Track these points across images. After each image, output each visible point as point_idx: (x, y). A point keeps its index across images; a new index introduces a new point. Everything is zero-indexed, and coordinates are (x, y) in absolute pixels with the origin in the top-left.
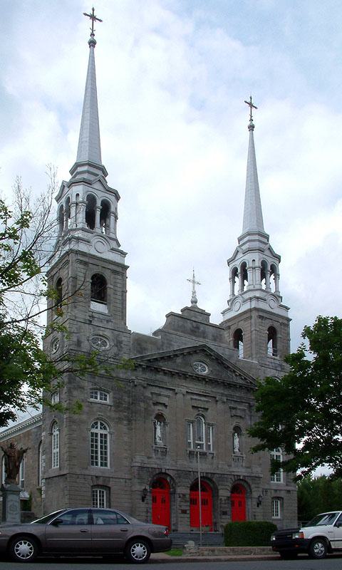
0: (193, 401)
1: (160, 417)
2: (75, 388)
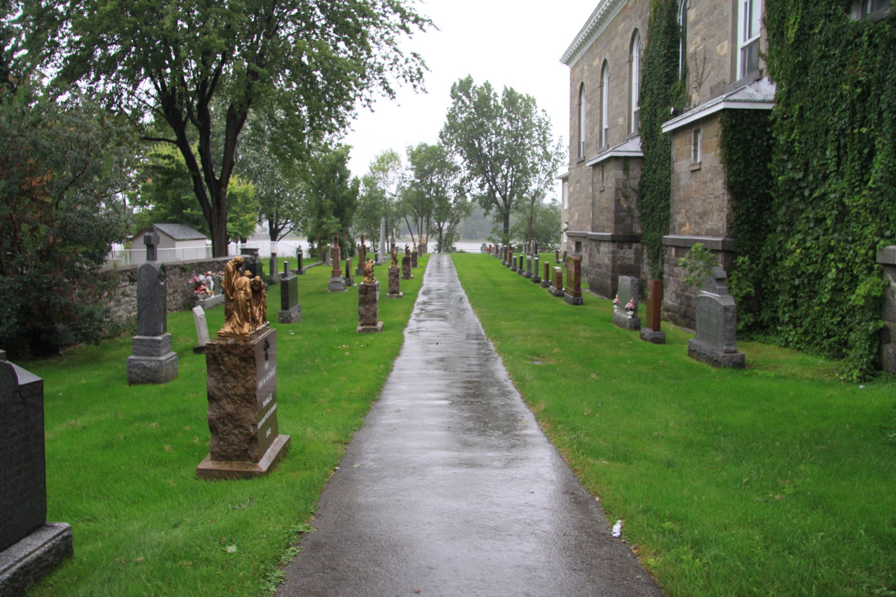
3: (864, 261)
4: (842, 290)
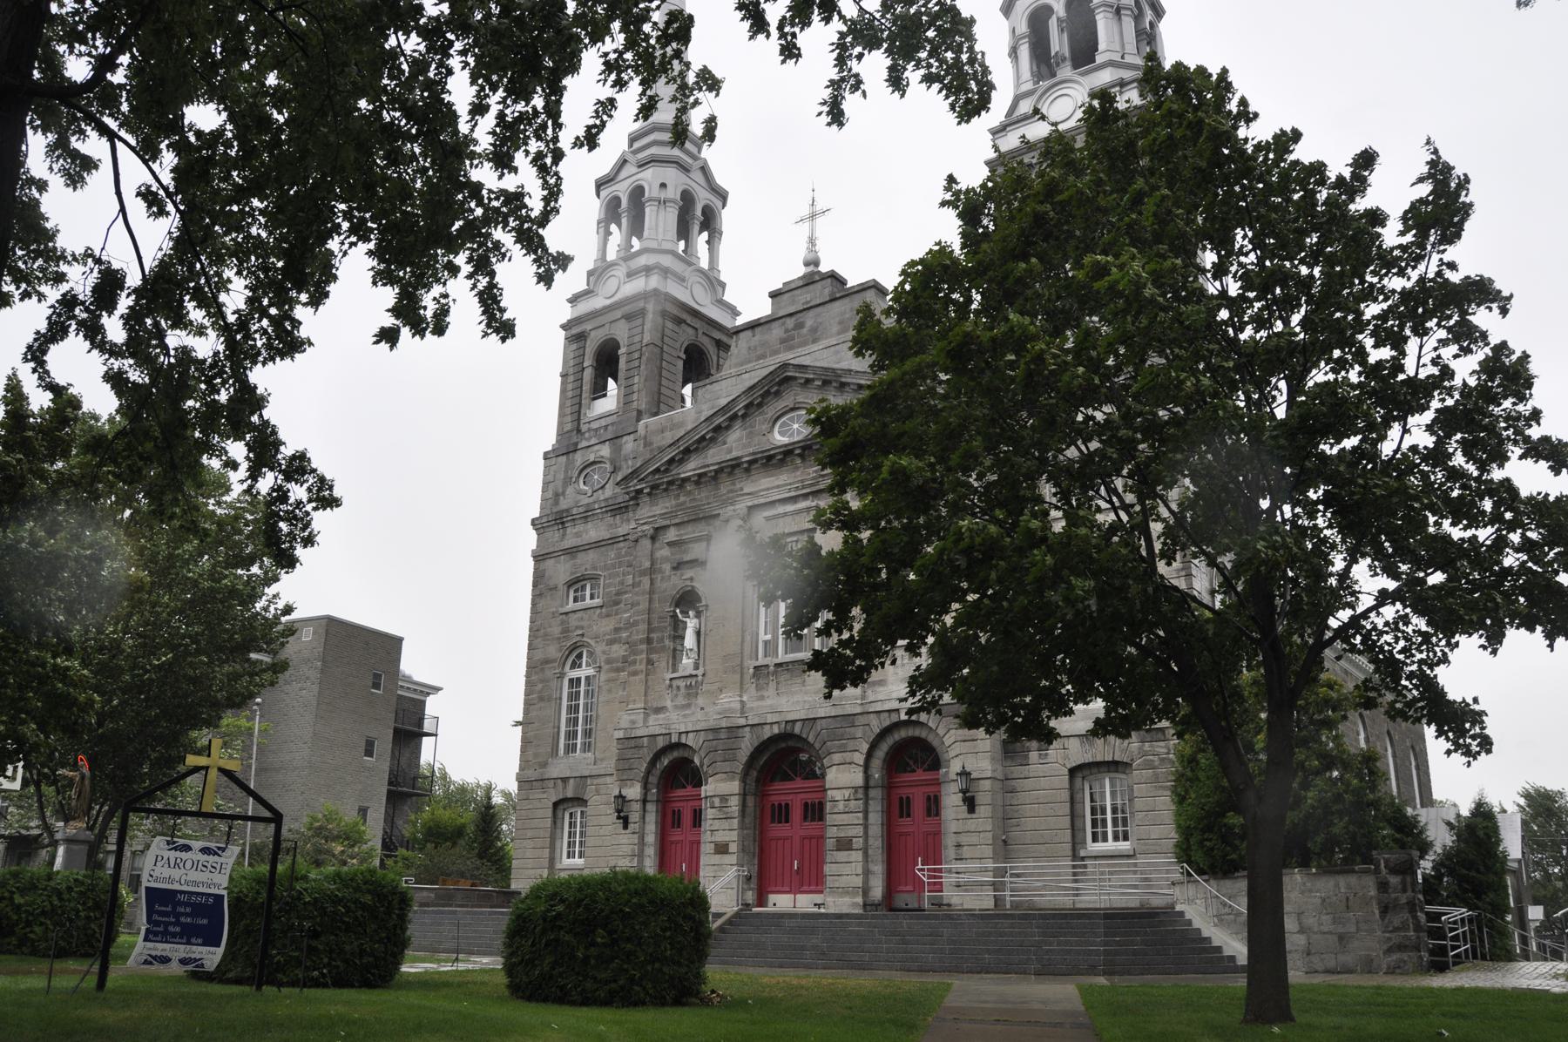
1: (687, 600)
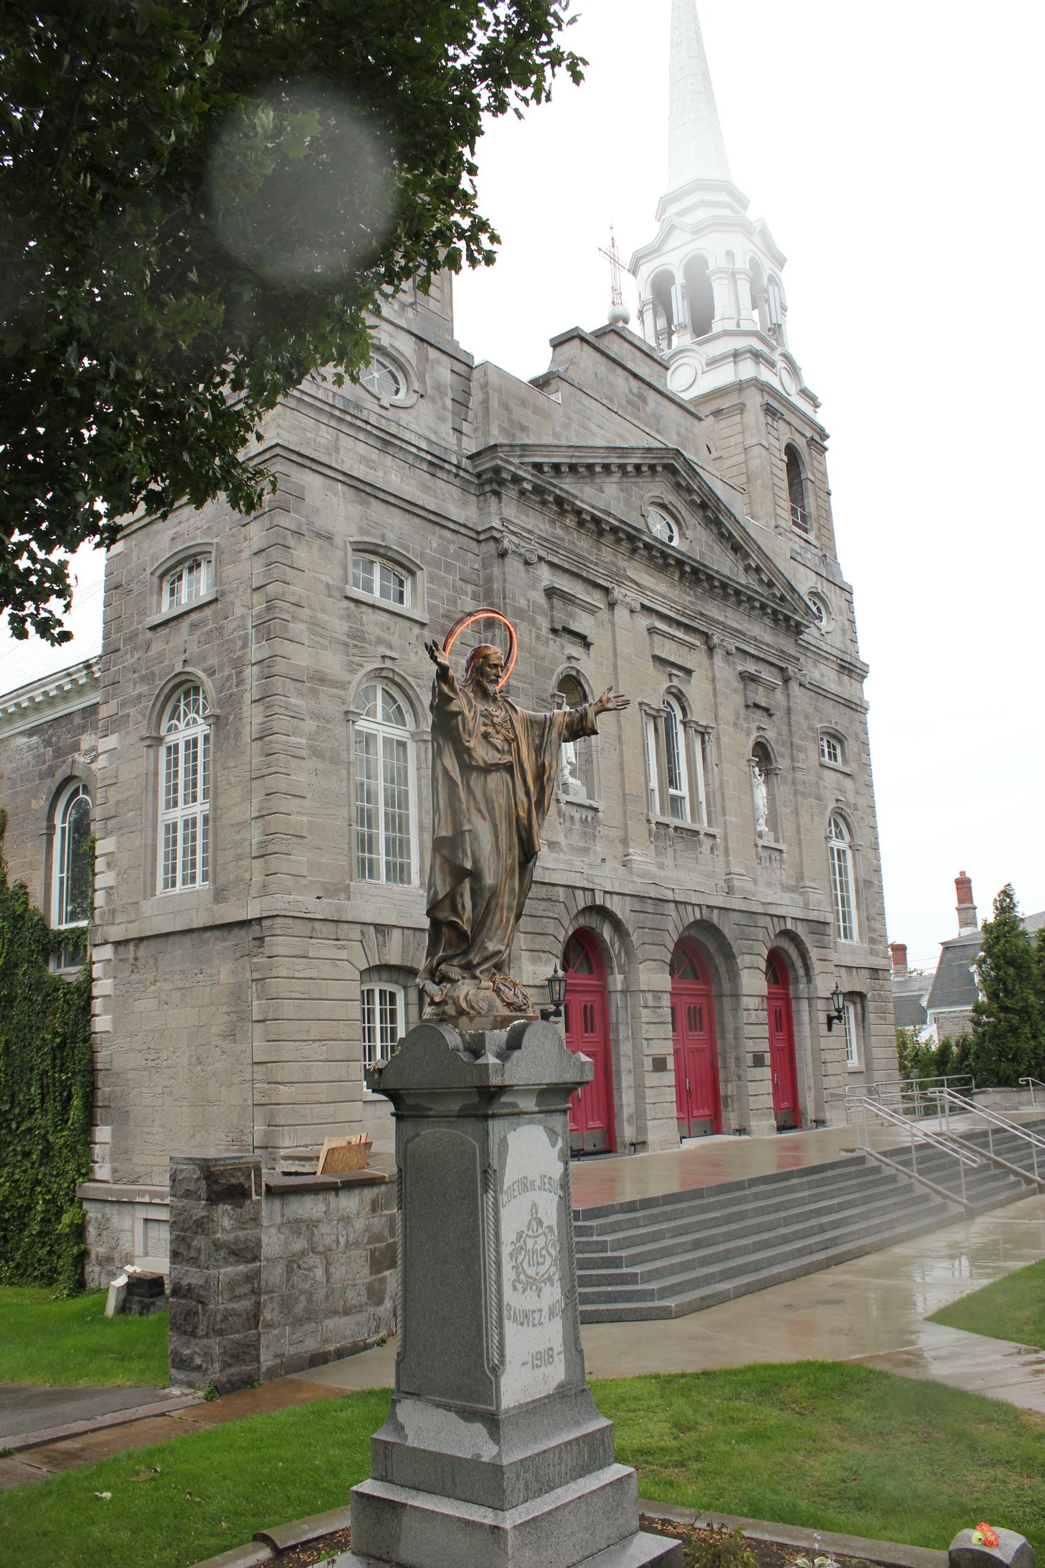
0: (656, 637)
2: (298, 534)
3: (67, 1194)
4: (49, 1221)
